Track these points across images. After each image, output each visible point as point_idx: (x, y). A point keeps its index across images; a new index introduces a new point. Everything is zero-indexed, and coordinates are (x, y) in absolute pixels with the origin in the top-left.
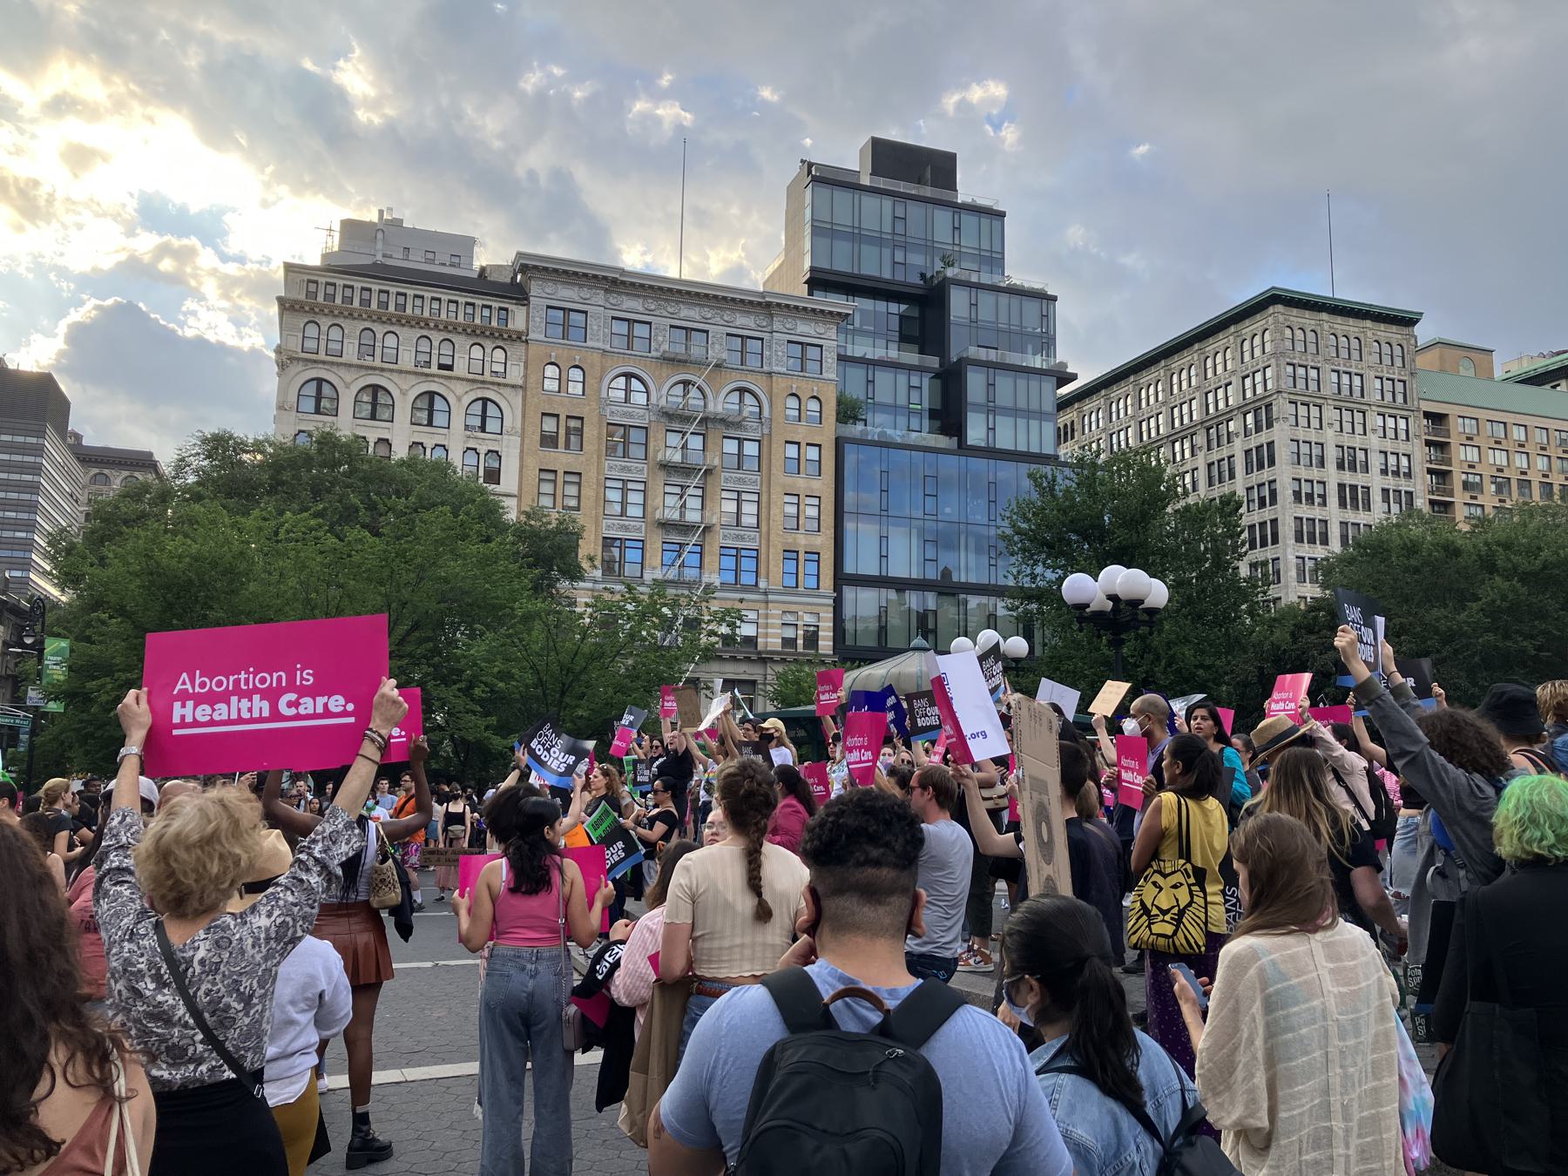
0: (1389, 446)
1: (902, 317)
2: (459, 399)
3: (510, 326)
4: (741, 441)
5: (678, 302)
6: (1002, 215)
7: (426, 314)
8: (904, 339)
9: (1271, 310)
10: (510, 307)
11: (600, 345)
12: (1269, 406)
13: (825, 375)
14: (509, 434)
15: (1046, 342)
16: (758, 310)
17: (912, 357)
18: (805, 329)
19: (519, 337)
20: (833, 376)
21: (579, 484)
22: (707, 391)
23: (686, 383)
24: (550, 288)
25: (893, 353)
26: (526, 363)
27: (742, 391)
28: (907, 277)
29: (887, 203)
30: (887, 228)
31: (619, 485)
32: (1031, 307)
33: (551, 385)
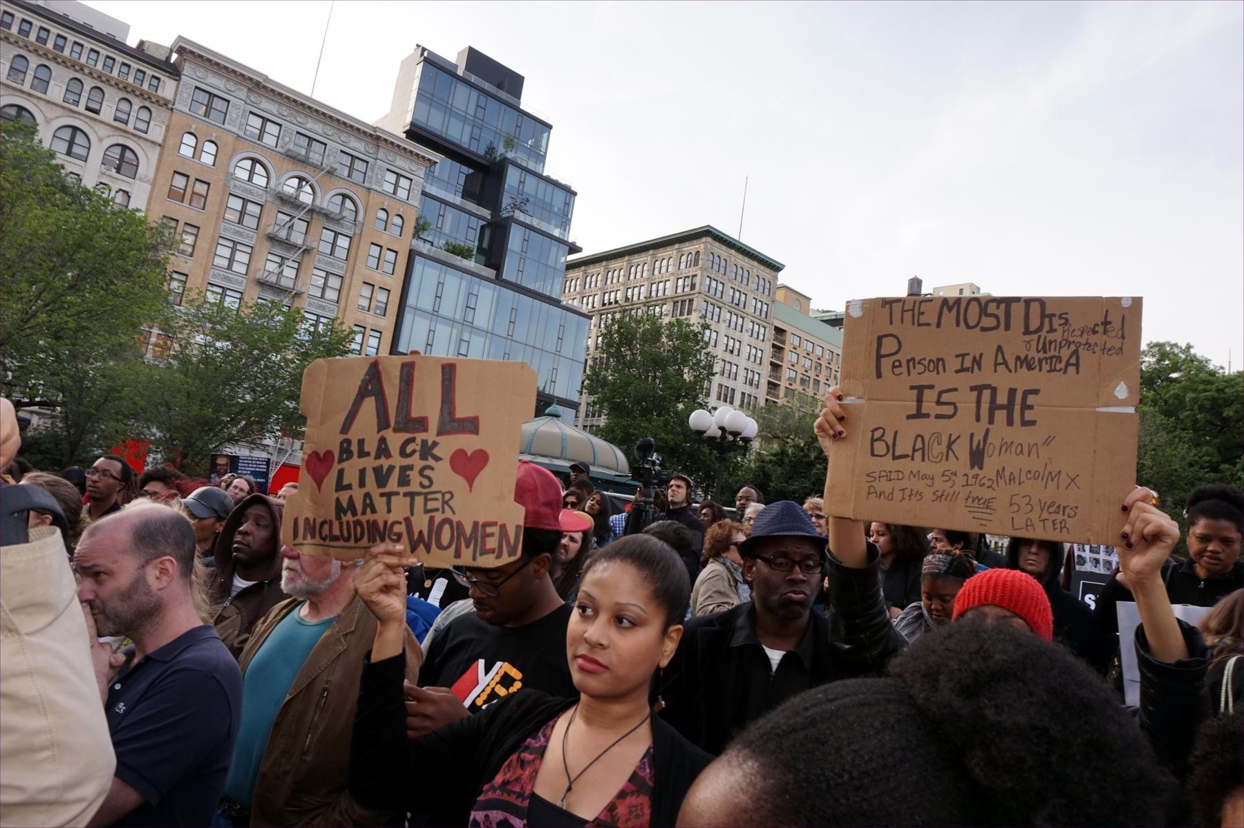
0: (753, 342)
1: (467, 176)
2: (101, 140)
3: (160, 93)
4: (337, 234)
5: (306, 116)
6: (550, 127)
7: (83, 60)
8: (466, 194)
9: (704, 239)
10: (163, 78)
11: (235, 130)
12: (691, 301)
13: (410, 202)
14: (141, 180)
15: (565, 221)
16: (369, 139)
18: (402, 163)
19: (165, 104)
20: (416, 204)
21: (196, 236)
23: (301, 179)
24: (200, 73)
25: (458, 200)
26: (168, 127)
27: (345, 196)
28: (476, 149)
29: (475, 94)
30: (471, 111)
31: (230, 244)
32: (560, 195)
33: (187, 151)
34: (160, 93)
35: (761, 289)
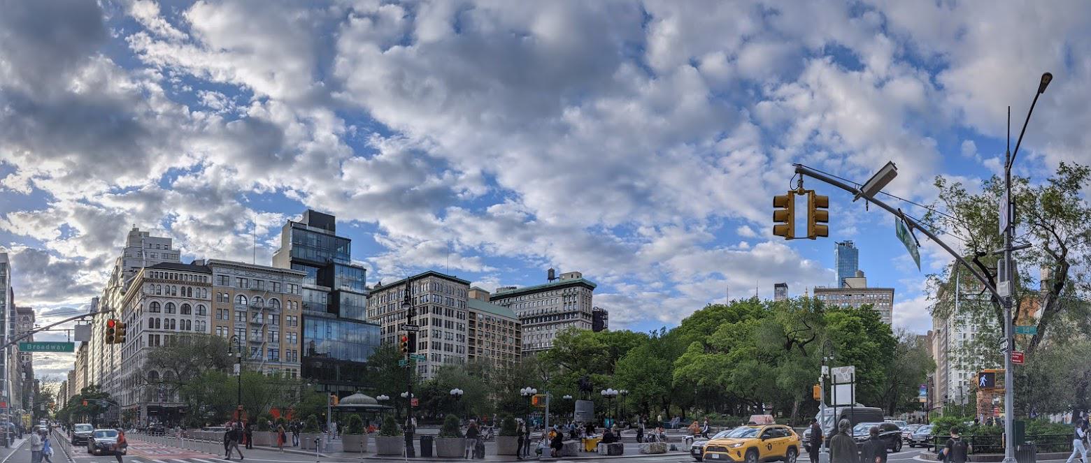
3: (207, 282)
12: (427, 307)
17: (322, 288)
19: (210, 285)
22: (264, 300)
32: (358, 272)
34: (207, 282)
35: (461, 295)
